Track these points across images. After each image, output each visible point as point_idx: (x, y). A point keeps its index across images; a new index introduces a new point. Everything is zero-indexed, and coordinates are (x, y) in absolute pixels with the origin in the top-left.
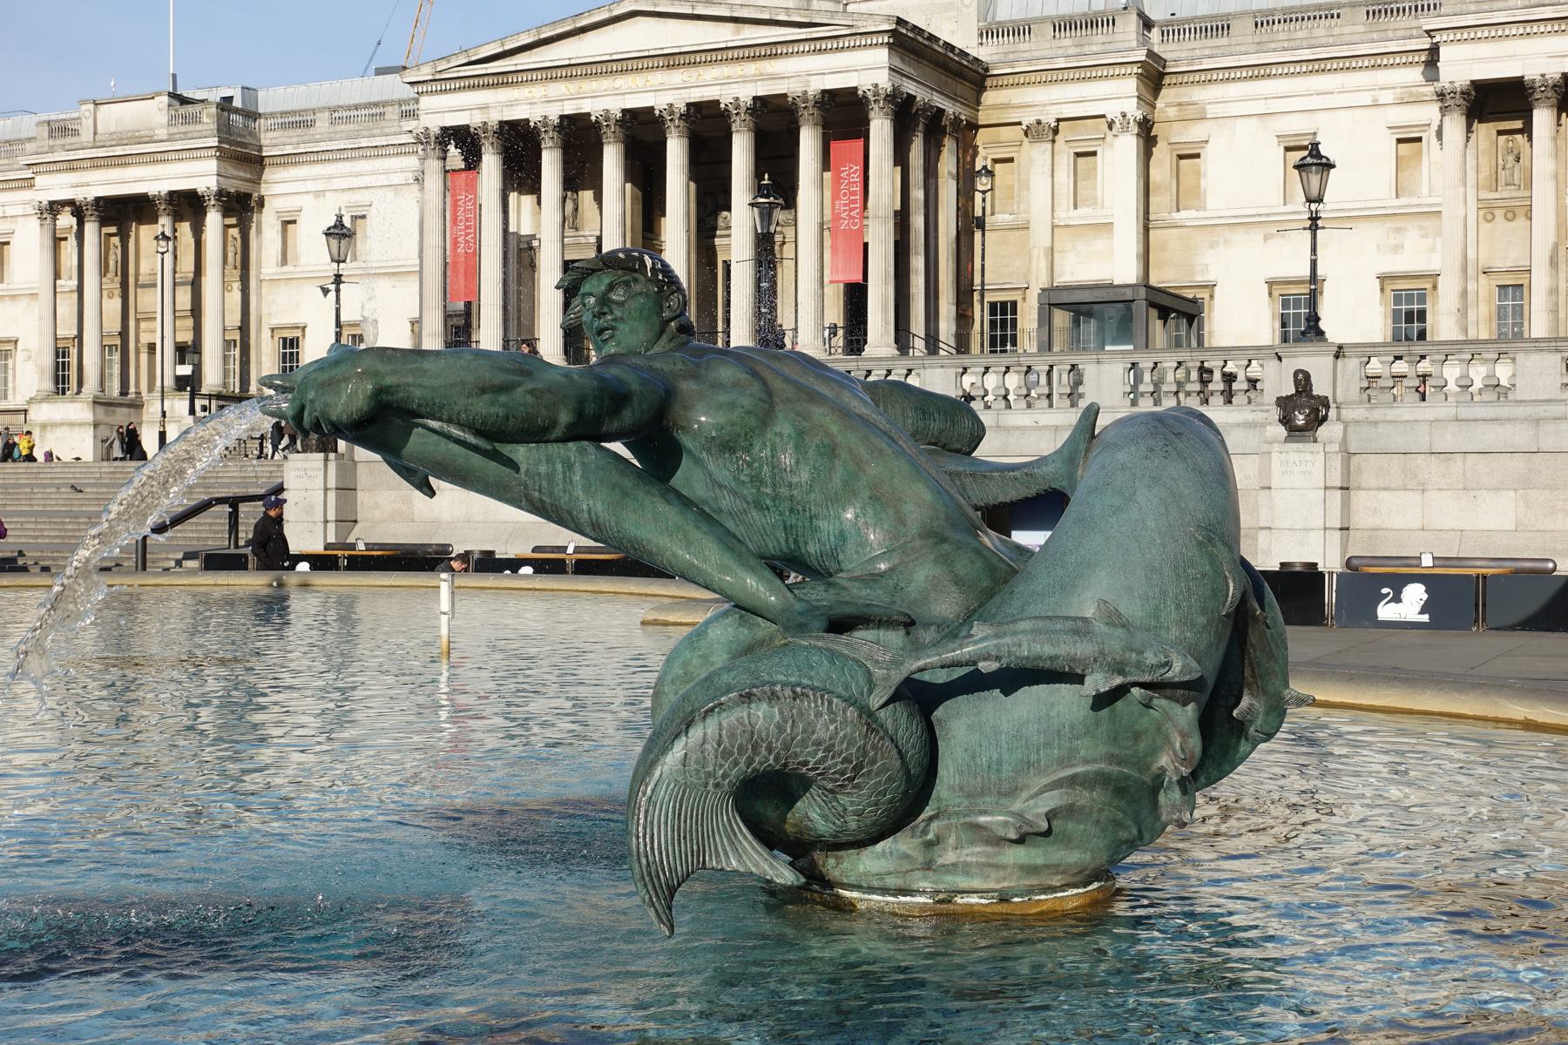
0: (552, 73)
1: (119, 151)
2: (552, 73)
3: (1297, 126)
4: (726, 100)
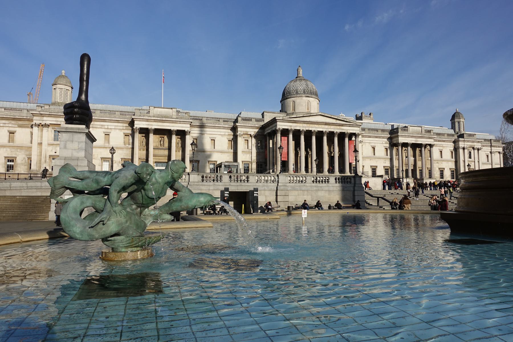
0: (305, 122)
1: (164, 119)
2: (305, 122)
3: (373, 145)
4: (335, 132)
